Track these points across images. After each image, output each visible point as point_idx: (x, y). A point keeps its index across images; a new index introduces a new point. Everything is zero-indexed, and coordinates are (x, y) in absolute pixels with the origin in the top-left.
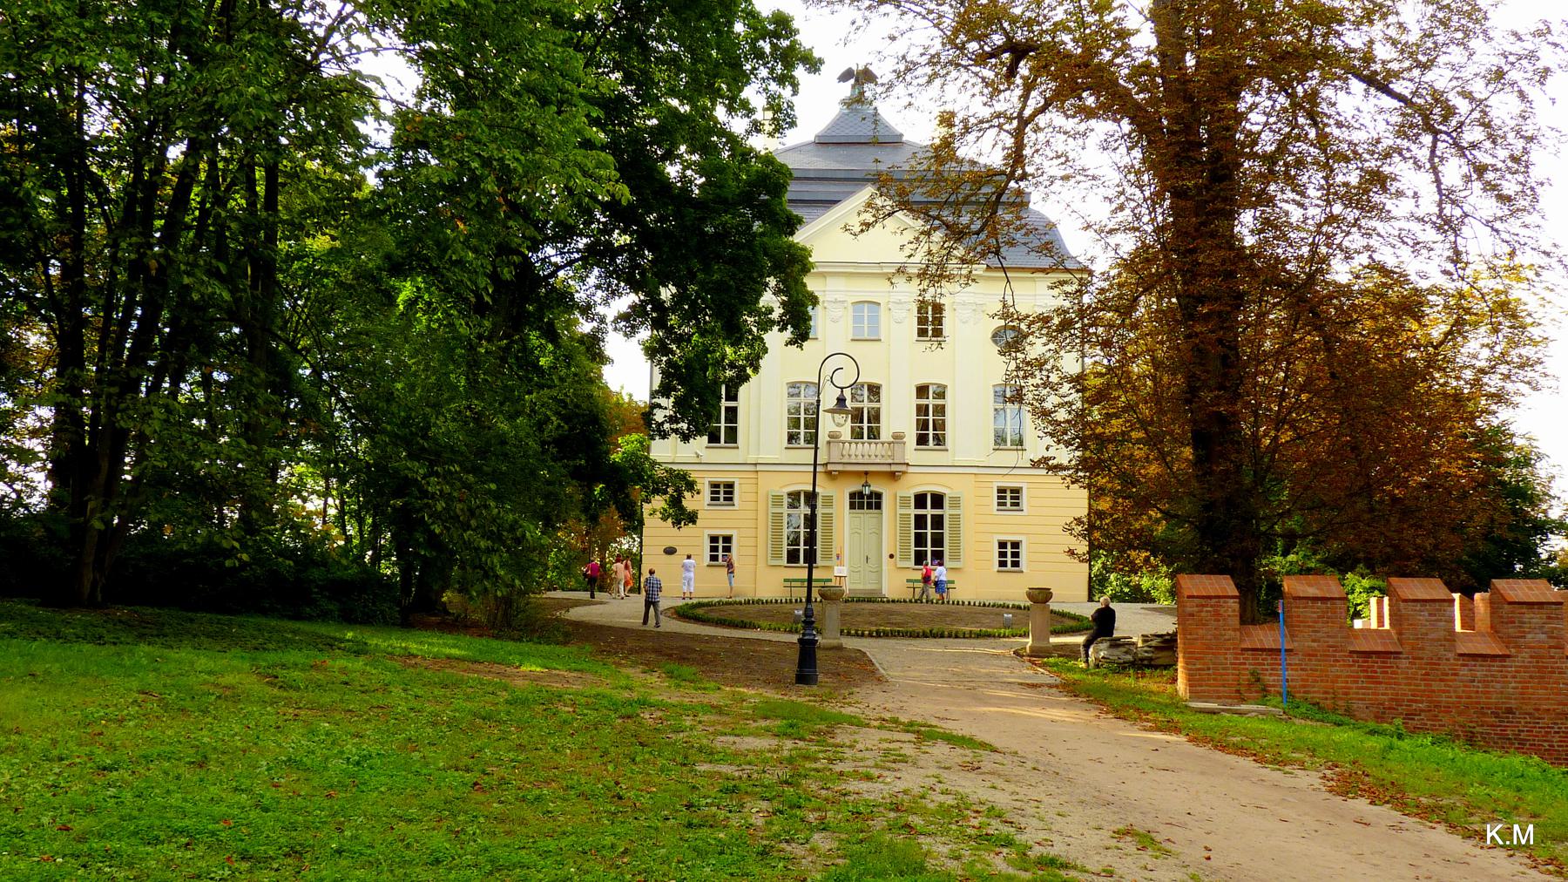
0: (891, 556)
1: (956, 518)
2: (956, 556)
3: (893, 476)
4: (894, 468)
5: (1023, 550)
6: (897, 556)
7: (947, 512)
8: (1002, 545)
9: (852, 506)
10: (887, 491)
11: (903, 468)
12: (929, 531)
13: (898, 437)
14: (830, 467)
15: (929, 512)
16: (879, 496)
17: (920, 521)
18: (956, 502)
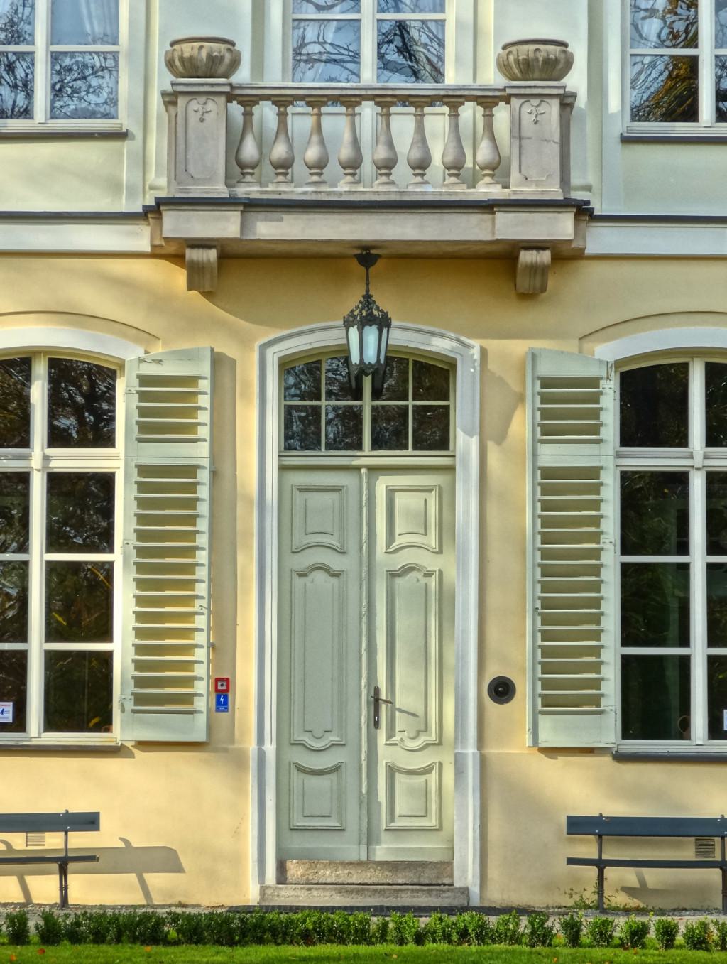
3: (506, 273)
4: (508, 227)
6: (525, 690)
9: (300, 432)
10: (490, 354)
11: (562, 226)
13: (538, 67)
14: (177, 224)
16: (435, 377)
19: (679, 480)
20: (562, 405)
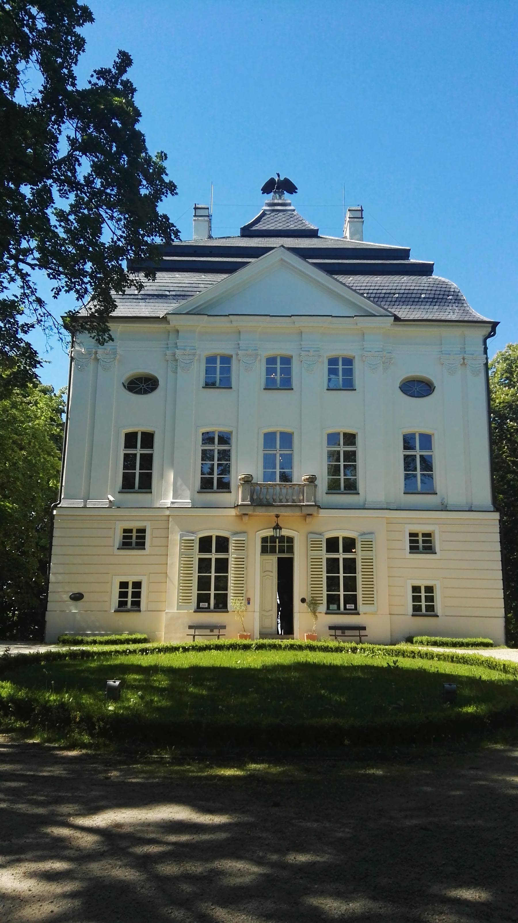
0: (303, 600)
1: (369, 562)
2: (370, 600)
5: (438, 595)
7: (359, 554)
8: (416, 589)
12: (341, 575)
15: (341, 556)
16: (290, 540)
17: (332, 565)
18: (368, 546)
19: (338, 559)
20: (314, 545)
